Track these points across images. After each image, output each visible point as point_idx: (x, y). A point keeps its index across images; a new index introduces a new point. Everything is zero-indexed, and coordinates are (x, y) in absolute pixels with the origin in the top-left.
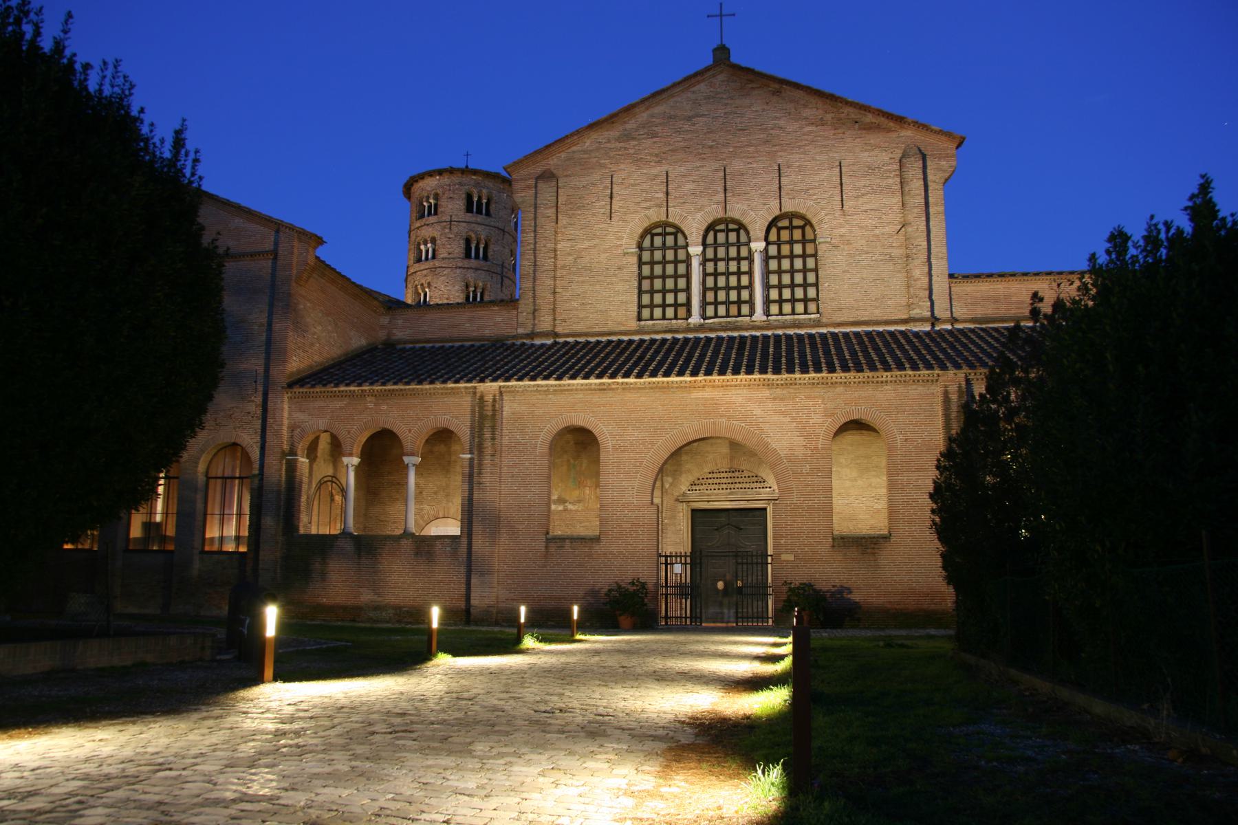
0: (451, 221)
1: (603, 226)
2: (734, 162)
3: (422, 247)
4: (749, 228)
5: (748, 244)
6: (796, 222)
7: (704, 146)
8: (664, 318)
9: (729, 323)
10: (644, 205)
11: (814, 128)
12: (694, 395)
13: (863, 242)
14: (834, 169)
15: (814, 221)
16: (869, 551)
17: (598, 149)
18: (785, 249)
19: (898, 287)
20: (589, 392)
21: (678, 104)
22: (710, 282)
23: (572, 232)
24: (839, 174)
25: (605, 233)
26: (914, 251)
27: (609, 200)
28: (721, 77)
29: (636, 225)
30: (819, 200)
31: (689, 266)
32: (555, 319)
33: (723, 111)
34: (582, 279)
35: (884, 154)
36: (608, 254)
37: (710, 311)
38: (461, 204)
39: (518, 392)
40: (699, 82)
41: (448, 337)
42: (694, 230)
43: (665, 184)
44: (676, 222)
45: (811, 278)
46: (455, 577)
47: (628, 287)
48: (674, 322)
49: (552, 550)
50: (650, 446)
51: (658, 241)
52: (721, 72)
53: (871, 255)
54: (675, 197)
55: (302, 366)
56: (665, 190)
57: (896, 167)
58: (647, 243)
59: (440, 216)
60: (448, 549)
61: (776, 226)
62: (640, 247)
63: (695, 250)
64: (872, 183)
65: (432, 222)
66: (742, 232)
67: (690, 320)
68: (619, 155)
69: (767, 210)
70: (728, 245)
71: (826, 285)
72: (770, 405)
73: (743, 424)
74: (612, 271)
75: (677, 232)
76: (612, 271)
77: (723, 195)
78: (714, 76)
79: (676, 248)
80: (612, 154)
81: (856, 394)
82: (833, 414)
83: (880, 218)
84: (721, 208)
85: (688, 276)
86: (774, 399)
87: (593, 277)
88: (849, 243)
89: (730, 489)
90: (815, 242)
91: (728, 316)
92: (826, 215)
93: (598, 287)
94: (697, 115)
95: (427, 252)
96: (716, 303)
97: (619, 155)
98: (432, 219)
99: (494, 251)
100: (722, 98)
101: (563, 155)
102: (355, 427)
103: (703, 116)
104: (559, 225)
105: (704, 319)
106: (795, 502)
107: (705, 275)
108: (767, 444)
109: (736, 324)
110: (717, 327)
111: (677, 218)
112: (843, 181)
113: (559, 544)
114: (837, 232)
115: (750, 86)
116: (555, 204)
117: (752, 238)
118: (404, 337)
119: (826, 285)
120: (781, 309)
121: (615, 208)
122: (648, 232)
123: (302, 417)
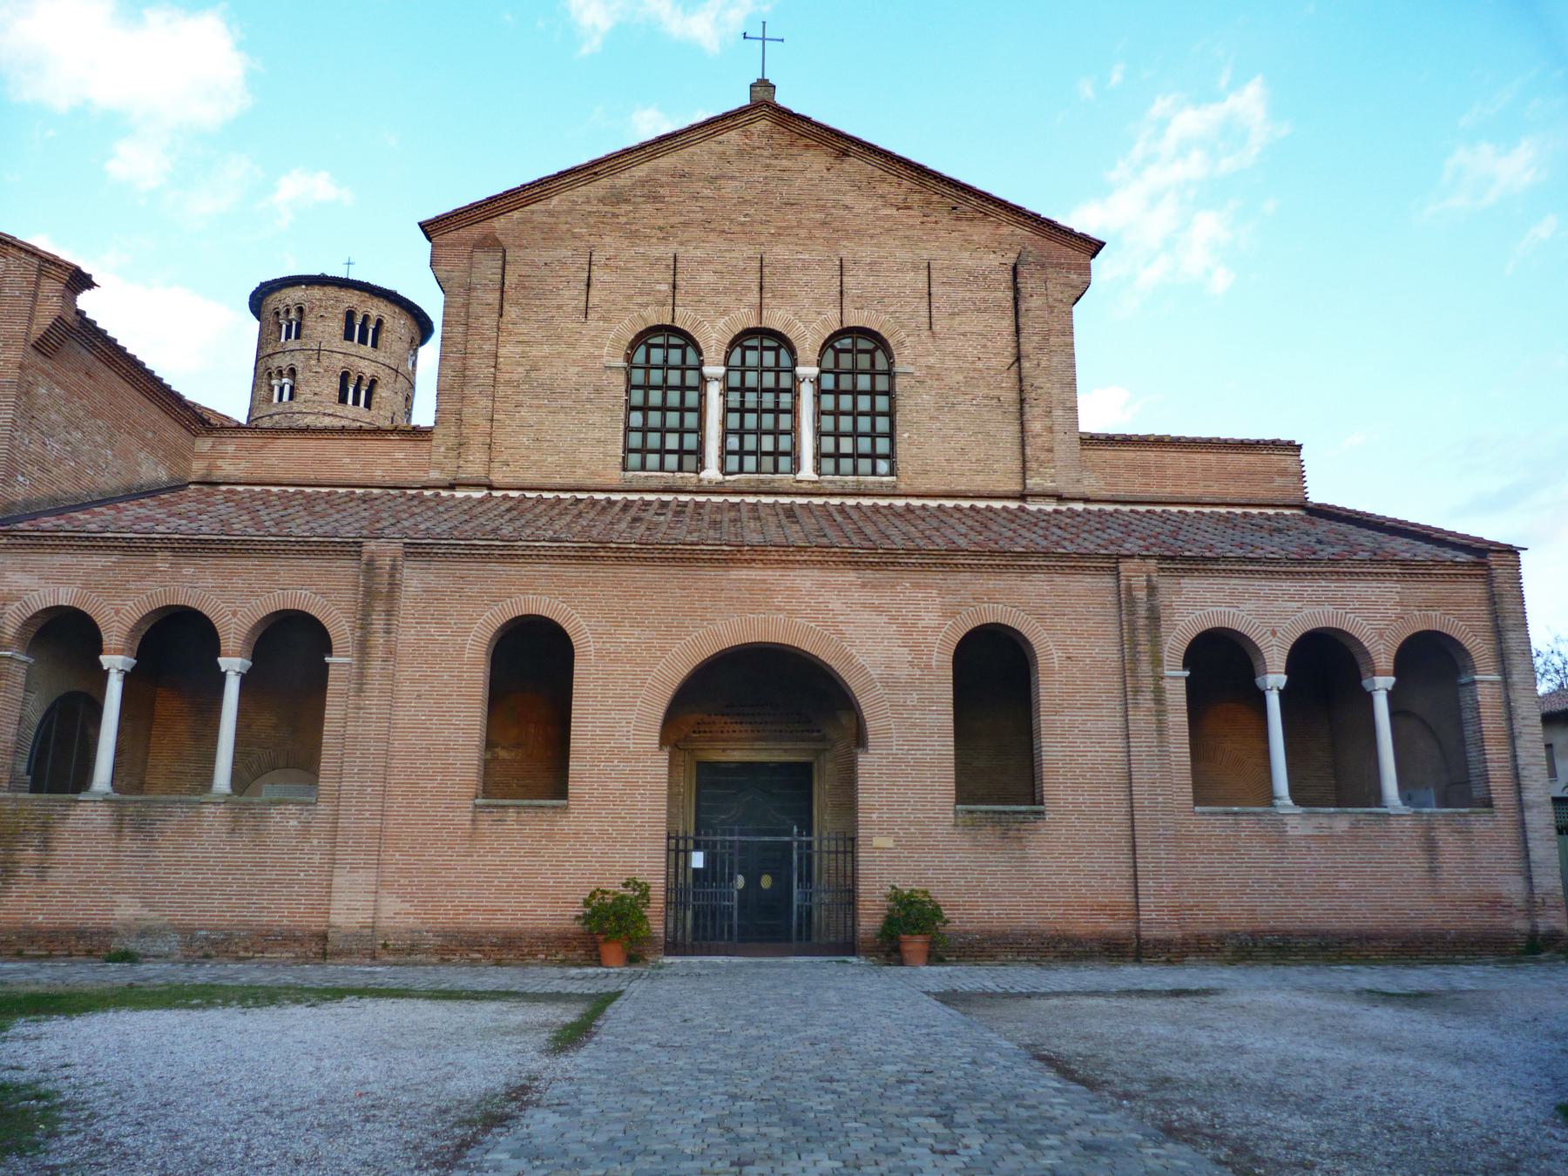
0: (319, 350)
1: (575, 325)
3: (274, 382)
4: (796, 344)
5: (791, 370)
6: (863, 344)
7: (732, 221)
8: (662, 468)
9: (762, 481)
10: (639, 300)
11: (894, 211)
13: (960, 378)
15: (891, 342)
16: (1011, 833)
17: (570, 212)
18: (846, 382)
19: (1009, 445)
21: (695, 157)
24: (926, 279)
25: (577, 337)
27: (584, 287)
28: (762, 125)
29: (628, 329)
30: (897, 315)
31: (703, 396)
32: (491, 461)
33: (764, 174)
34: (535, 402)
35: (992, 256)
36: (577, 369)
37: (733, 462)
38: (337, 326)
40: (729, 129)
41: (312, 477)
43: (672, 272)
44: (686, 329)
46: (302, 874)
49: (484, 826)
50: (659, 654)
51: (657, 356)
53: (970, 397)
54: (686, 292)
55: (35, 496)
56: (671, 281)
57: (1009, 276)
58: (640, 357)
59: (304, 340)
60: (293, 823)
61: (833, 347)
62: (631, 366)
63: (714, 370)
64: (974, 296)
65: (292, 348)
66: (783, 352)
67: (703, 475)
68: (603, 223)
69: (822, 322)
70: (761, 369)
71: (906, 435)
72: (856, 595)
73: (812, 624)
74: (584, 394)
76: (584, 394)
77: (758, 296)
78: (751, 121)
79: (683, 368)
80: (591, 220)
81: (991, 584)
82: (954, 614)
83: (984, 346)
84: (754, 313)
85: (700, 410)
86: (864, 586)
87: (555, 400)
88: (939, 378)
89: (758, 731)
91: (758, 471)
92: (908, 336)
93: (562, 416)
94: (723, 177)
96: (742, 453)
98: (293, 344)
99: (381, 397)
101: (516, 215)
102: (131, 603)
103: (732, 178)
104: (504, 319)
105: (724, 475)
106: (894, 752)
107: (727, 410)
109: (772, 484)
110: (744, 487)
111: (688, 323)
112: (933, 290)
113: (496, 816)
114: (922, 361)
118: (236, 473)
119: (906, 435)
121: (593, 300)
122: (643, 338)
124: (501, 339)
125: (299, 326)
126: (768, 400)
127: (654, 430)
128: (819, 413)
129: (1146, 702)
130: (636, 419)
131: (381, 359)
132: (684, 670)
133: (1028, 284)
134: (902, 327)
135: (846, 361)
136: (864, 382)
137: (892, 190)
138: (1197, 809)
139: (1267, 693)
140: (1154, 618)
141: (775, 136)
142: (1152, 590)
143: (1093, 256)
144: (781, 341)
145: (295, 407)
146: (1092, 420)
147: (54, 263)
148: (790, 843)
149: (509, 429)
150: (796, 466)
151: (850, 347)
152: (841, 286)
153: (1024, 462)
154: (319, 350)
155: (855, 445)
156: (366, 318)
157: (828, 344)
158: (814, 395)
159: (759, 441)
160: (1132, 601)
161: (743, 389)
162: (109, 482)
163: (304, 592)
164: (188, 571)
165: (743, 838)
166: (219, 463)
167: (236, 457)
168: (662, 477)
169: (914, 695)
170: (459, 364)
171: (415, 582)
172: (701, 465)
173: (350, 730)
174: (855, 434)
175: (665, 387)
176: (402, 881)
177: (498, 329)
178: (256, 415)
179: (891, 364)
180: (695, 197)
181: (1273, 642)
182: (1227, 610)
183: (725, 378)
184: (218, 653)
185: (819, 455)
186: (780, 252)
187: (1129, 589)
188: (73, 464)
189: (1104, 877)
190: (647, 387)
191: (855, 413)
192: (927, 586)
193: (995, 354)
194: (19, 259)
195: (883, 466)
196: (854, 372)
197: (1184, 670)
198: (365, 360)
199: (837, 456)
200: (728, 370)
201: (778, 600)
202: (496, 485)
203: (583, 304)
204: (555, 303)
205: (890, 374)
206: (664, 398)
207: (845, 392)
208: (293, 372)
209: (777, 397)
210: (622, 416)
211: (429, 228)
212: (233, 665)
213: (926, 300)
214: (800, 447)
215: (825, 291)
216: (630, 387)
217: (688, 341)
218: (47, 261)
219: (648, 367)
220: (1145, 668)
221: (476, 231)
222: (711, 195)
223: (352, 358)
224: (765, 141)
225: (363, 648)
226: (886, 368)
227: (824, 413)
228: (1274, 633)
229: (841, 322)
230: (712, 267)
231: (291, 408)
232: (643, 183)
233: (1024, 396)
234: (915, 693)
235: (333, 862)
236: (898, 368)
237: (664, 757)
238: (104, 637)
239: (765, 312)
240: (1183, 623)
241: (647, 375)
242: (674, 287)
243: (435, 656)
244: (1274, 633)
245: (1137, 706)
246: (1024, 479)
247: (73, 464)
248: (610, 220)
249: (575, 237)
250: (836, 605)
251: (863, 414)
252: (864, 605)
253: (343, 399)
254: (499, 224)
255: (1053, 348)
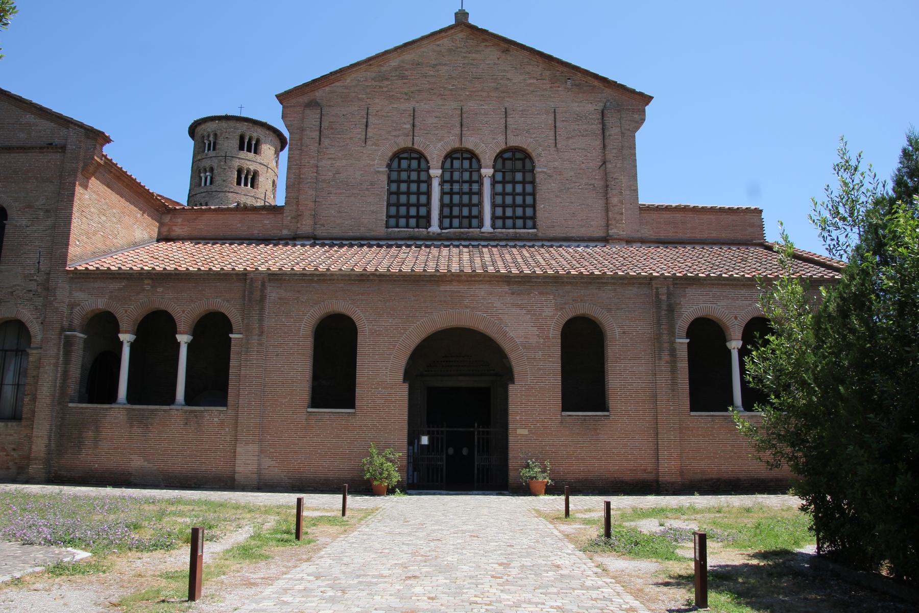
0: (226, 156)
1: (359, 148)
2: (469, 104)
3: (202, 175)
4: (481, 157)
5: (479, 171)
6: (518, 155)
7: (445, 88)
8: (407, 226)
9: (462, 233)
10: (394, 133)
11: (535, 81)
12: (442, 288)
14: (550, 114)
15: (534, 155)
20: (349, 282)
22: (447, 199)
23: (332, 152)
24: (553, 119)
26: (613, 183)
27: (364, 127)
28: (460, 35)
29: (388, 149)
30: (537, 139)
32: (315, 224)
35: (590, 105)
36: (362, 172)
37: (446, 222)
38: (236, 143)
39: (285, 280)
40: (442, 38)
41: (222, 234)
42: (435, 156)
43: (412, 118)
45: (529, 200)
46: (221, 446)
47: (378, 200)
48: (416, 230)
50: (402, 331)
51: (404, 164)
52: (462, 31)
53: (578, 184)
54: (420, 129)
56: (412, 122)
57: (599, 116)
59: (217, 151)
60: (216, 419)
61: (502, 157)
63: (436, 172)
66: (474, 160)
67: (430, 230)
68: (374, 91)
70: (463, 170)
71: (542, 206)
73: (485, 315)
75: (421, 157)
77: (459, 130)
80: (368, 90)
82: (562, 309)
83: (586, 156)
84: (457, 139)
85: (428, 194)
86: (513, 294)
88: (560, 173)
90: (533, 172)
92: (543, 150)
95: (206, 179)
96: (451, 217)
97: (374, 91)
98: (212, 153)
100: (461, 52)
101: (327, 89)
102: (132, 307)
104: (322, 146)
105: (441, 229)
107: (443, 193)
108: (505, 334)
111: (421, 146)
112: (557, 124)
115: (485, 44)
116: (318, 128)
117: (483, 165)
118: (183, 233)
119: (542, 206)
120: (504, 223)
121: (369, 135)
122: (397, 156)
123: (82, 296)
124: (320, 157)
125: (215, 143)
126: (466, 187)
127: (403, 205)
128: (494, 194)
129: (666, 357)
130: (394, 199)
131: (258, 161)
132: (417, 341)
133: (611, 121)
134: (540, 146)
135: (509, 164)
136: (519, 176)
137: (534, 69)
138: (693, 413)
139: (732, 351)
140: (671, 310)
141: (468, 41)
142: (669, 295)
143: (647, 104)
144: (472, 156)
145: (213, 188)
146: (646, 198)
147: (91, 131)
148: (473, 432)
149: (324, 206)
150: (481, 225)
151: (511, 157)
152: (506, 123)
153: (608, 221)
154: (226, 156)
155: (514, 212)
156: (250, 139)
157: (500, 156)
158: (491, 184)
159: (461, 211)
160: (658, 301)
161: (452, 182)
162: (119, 242)
163: (218, 300)
164: (160, 290)
165: (448, 429)
166: (174, 228)
167: (183, 225)
168: (407, 231)
169: (540, 353)
170: (298, 171)
171: (274, 295)
172: (428, 224)
173: (243, 372)
174: (514, 206)
175: (409, 181)
176: (271, 450)
177: (318, 151)
178: (193, 193)
179: (534, 167)
180: (425, 76)
181: (736, 323)
182: (711, 305)
183: (442, 176)
184: (176, 333)
185: (494, 218)
186: (471, 105)
187: (657, 294)
188: (102, 234)
189: (640, 450)
190: (399, 181)
191: (514, 194)
192: (547, 293)
193: (591, 160)
194: (75, 129)
195: (529, 223)
196: (513, 171)
197: (687, 338)
198: (248, 161)
199: (504, 218)
200: (443, 172)
201: (466, 302)
202: (318, 237)
203: (363, 137)
204: (348, 136)
205: (532, 171)
206: (408, 188)
207: (509, 182)
208: (212, 170)
209: (470, 185)
210: (386, 198)
211: (282, 98)
212: (184, 339)
213: (553, 130)
214: (483, 214)
215: (497, 126)
216: (390, 181)
217: (421, 157)
218: (88, 130)
219: (399, 170)
220: (665, 337)
221: (306, 99)
222: (433, 74)
223: (243, 161)
224: (463, 44)
225: (248, 330)
226: (531, 168)
227: (497, 194)
228: (736, 318)
229: (506, 143)
230: (434, 114)
231: (211, 189)
232: (396, 69)
233: (608, 183)
234: (540, 352)
235: (236, 440)
236: (538, 170)
237: (406, 386)
238: (120, 324)
239: (463, 139)
240: (686, 313)
241: (399, 175)
242: (414, 126)
243: (285, 333)
244: (736, 318)
245: (660, 359)
246: (608, 231)
247: (102, 234)
248: (378, 90)
249: (359, 99)
250: (498, 304)
251: (519, 194)
252: (513, 305)
253: (239, 183)
254: (319, 94)
255: (624, 157)
